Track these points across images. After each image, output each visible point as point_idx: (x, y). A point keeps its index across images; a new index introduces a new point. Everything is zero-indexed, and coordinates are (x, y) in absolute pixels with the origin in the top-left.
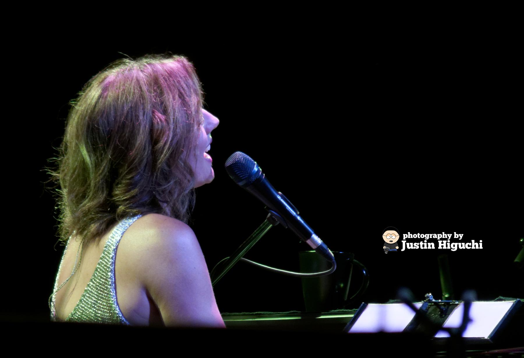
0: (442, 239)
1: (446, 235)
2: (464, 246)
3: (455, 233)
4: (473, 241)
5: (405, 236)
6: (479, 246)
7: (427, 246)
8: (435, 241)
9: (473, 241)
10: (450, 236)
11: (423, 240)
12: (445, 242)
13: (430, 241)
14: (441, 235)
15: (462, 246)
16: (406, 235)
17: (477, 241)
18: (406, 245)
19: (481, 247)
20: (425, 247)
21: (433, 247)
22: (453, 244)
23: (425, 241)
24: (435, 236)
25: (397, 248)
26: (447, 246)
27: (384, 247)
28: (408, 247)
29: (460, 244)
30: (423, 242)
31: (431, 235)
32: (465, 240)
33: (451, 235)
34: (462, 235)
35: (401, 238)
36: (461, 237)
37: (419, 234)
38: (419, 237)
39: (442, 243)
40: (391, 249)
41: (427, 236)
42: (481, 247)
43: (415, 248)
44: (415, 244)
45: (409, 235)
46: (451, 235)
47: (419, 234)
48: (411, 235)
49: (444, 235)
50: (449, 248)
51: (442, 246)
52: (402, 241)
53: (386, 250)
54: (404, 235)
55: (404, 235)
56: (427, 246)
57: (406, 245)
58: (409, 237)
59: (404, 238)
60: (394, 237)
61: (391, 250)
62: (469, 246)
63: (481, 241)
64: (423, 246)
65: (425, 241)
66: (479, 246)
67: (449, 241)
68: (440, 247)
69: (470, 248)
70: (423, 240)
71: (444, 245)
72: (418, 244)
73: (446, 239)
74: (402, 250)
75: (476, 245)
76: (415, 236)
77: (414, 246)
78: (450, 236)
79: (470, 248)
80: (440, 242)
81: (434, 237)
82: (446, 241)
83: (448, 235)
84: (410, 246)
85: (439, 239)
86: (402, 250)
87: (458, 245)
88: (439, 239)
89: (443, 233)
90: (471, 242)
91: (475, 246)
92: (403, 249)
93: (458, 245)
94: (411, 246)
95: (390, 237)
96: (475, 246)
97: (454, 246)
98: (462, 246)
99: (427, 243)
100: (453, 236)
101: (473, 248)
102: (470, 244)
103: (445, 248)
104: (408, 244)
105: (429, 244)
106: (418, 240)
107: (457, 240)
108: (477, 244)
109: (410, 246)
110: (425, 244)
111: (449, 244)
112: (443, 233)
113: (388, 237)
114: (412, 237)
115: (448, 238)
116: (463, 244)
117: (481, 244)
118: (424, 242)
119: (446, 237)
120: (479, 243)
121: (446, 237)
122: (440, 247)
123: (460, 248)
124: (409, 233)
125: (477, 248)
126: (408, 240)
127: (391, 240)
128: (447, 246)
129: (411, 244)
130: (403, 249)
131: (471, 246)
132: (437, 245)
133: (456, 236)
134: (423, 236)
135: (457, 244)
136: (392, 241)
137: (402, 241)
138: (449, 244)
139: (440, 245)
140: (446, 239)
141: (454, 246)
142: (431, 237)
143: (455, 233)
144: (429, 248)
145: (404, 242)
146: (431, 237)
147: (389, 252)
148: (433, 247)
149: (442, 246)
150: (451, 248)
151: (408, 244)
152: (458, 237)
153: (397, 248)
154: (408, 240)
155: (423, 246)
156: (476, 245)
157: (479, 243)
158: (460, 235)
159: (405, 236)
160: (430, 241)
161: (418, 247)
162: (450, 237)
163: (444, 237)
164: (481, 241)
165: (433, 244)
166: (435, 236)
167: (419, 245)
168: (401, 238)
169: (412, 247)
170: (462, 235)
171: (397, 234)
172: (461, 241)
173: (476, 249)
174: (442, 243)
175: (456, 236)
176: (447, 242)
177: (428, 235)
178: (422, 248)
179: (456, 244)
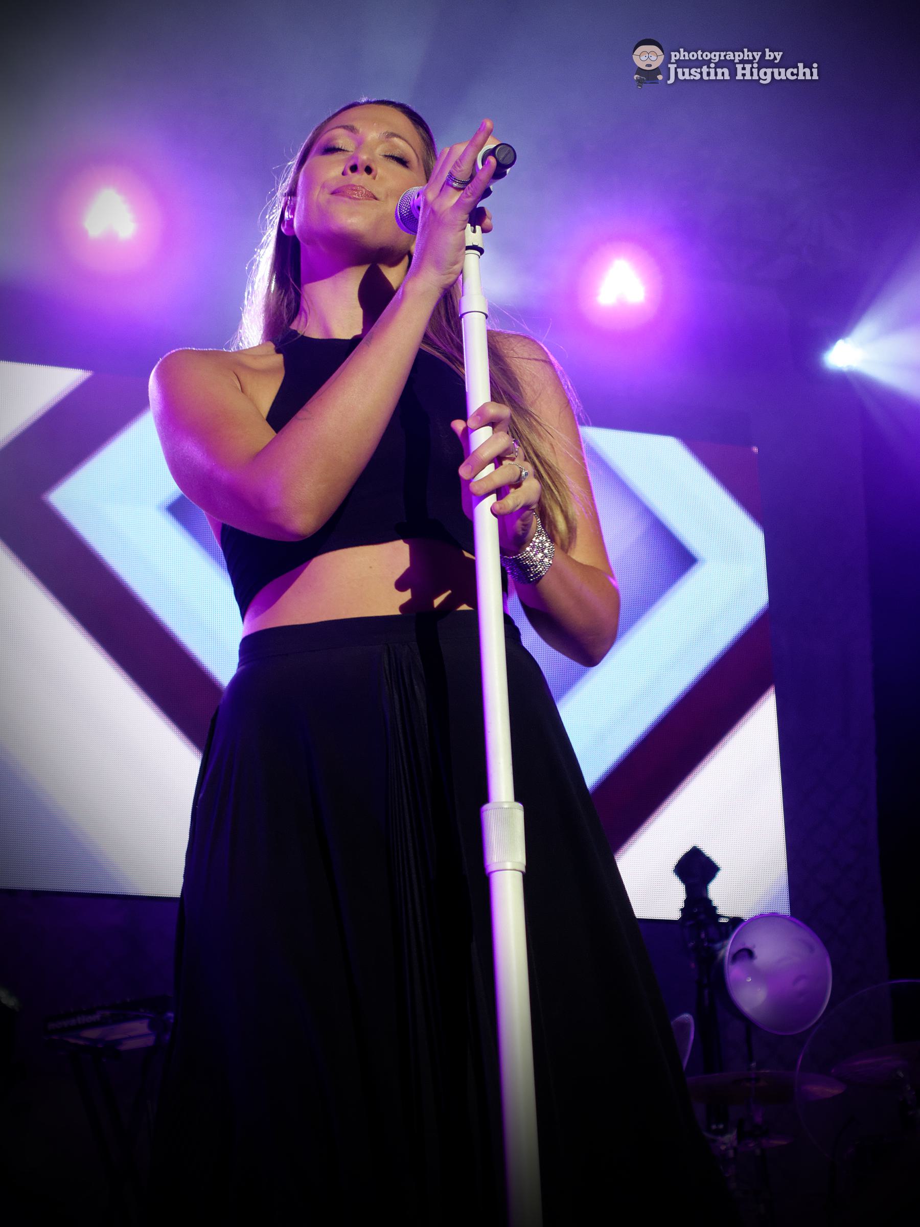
19: (815, 77)
20: (712, 77)
21: (727, 77)
28: (681, 77)
43: (692, 77)
50: (755, 77)
53: (638, 81)
68: (739, 77)
69: (795, 77)
74: (669, 82)
79: (795, 77)
86: (669, 82)
92: (672, 80)
101: (801, 77)
103: (748, 77)
123: (777, 77)
125: (808, 77)
130: (672, 80)
144: (720, 77)
150: (760, 78)
161: (698, 77)
169: (687, 77)
178: (705, 77)
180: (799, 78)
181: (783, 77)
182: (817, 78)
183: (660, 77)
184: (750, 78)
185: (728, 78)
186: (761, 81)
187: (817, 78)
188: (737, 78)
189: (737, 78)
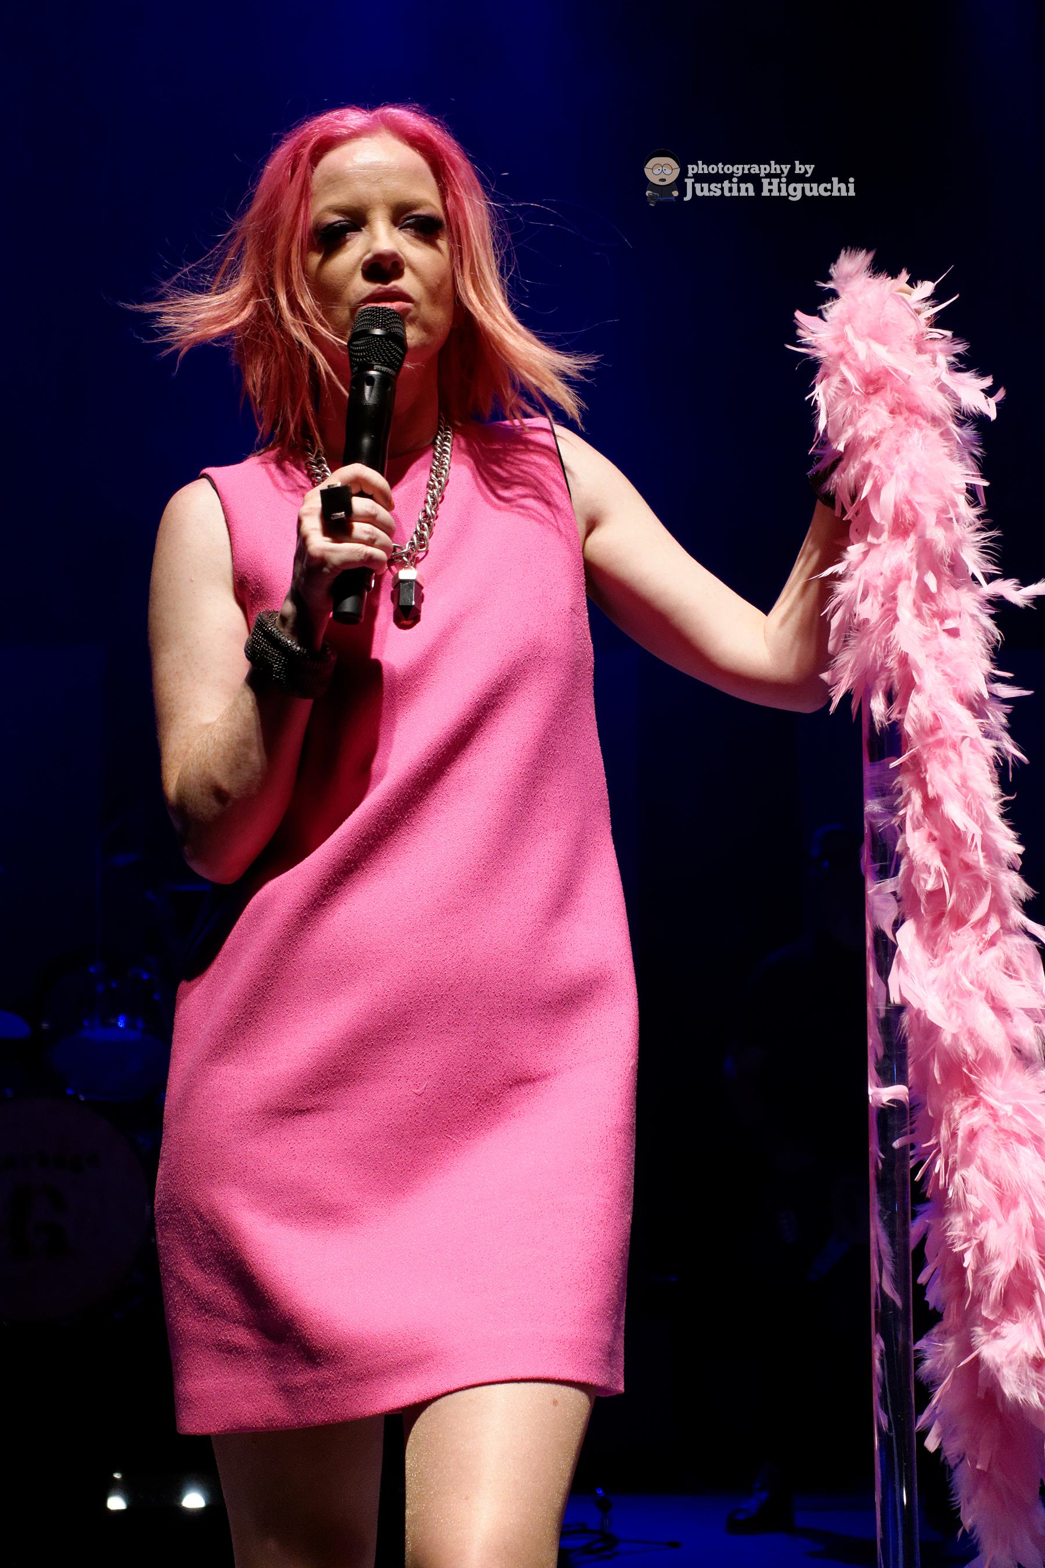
0: (769, 176)
1: (778, 166)
2: (816, 190)
3: (797, 162)
4: (835, 180)
6: (848, 190)
7: (739, 190)
8: (755, 180)
9: (835, 180)
10: (786, 168)
11: (729, 177)
12: (775, 181)
13: (744, 179)
14: (767, 167)
15: (811, 190)
16: (695, 166)
17: (844, 180)
19: (852, 193)
20: (735, 193)
21: (752, 193)
22: (792, 186)
23: (735, 180)
24: (755, 169)
25: (676, 193)
26: (780, 190)
27: (648, 193)
28: (699, 193)
29: (807, 186)
30: (730, 182)
31: (747, 167)
32: (818, 178)
33: (789, 166)
34: (813, 166)
35: (684, 173)
36: (810, 171)
37: (720, 165)
38: (721, 172)
39: (770, 184)
40: (661, 196)
41: (738, 170)
42: (852, 193)
43: (712, 194)
44: (713, 186)
45: (701, 168)
46: (789, 166)
47: (720, 165)
48: (705, 166)
49: (774, 167)
50: (784, 193)
51: (770, 191)
52: (686, 180)
53: (651, 197)
54: (690, 167)
55: (690, 167)
56: (739, 190)
58: (700, 172)
59: (690, 173)
60: (668, 171)
61: (662, 199)
62: (826, 190)
63: (852, 180)
64: (730, 190)
65: (735, 180)
66: (848, 190)
67: (784, 180)
68: (765, 193)
69: (829, 193)
70: (729, 177)
71: (775, 187)
72: (719, 185)
73: (778, 176)
74: (686, 199)
75: (841, 189)
77: (710, 190)
78: (786, 168)
79: (829, 193)
80: (765, 181)
81: (752, 171)
82: (778, 180)
83: (783, 167)
84: (702, 190)
85: (762, 175)
86: (686, 199)
87: (803, 189)
88: (762, 175)
89: (773, 162)
90: (832, 182)
91: (839, 190)
92: (688, 197)
93: (803, 189)
94: (704, 190)
95: (661, 170)
96: (839, 190)
97: (795, 189)
98: (811, 190)
99: (738, 183)
100: (793, 169)
101: (835, 193)
102: (829, 186)
103: (775, 193)
104: (698, 186)
105: (743, 186)
106: (719, 178)
107: (801, 179)
108: (843, 186)
109: (702, 190)
110: (735, 186)
111: (783, 186)
112: (773, 162)
113: (656, 171)
114: (706, 172)
115: (782, 172)
116: (814, 186)
117: (851, 186)
118: (731, 182)
119: (779, 171)
120: (847, 183)
121: (779, 171)
122: (765, 193)
123: (808, 193)
124: (700, 162)
125: (844, 193)
126: (699, 178)
127: (663, 176)
128: (780, 190)
129: (705, 186)
130: (688, 197)
131: (831, 191)
132: (758, 188)
133: (799, 168)
134: (729, 169)
135: (801, 185)
136: (663, 180)
137: (686, 180)
138: (783, 186)
140: (778, 176)
141: (795, 189)
142: (746, 171)
143: (797, 162)
144: (743, 193)
145: (689, 182)
146: (746, 171)
147: (658, 203)
149: (770, 191)
150: (789, 195)
152: (803, 171)
153: (676, 193)
154: (699, 178)
155: (730, 190)
156: (841, 189)
157: (847, 183)
158: (807, 166)
160: (744, 179)
161: (719, 193)
162: (786, 171)
163: (773, 171)
165: (750, 186)
166: (755, 169)
167: (722, 189)
168: (684, 173)
169: (706, 193)
170: (813, 166)
172: (810, 180)
173: (840, 197)
174: (770, 184)
175: (799, 168)
176: (781, 182)
177: (741, 167)
178: (727, 194)
179: (799, 186)
180: (834, 194)
181: (815, 193)
182: (853, 194)
184: (778, 194)
185: (753, 194)
186: (790, 198)
187: (853, 194)
188: (763, 194)
189: (763, 194)
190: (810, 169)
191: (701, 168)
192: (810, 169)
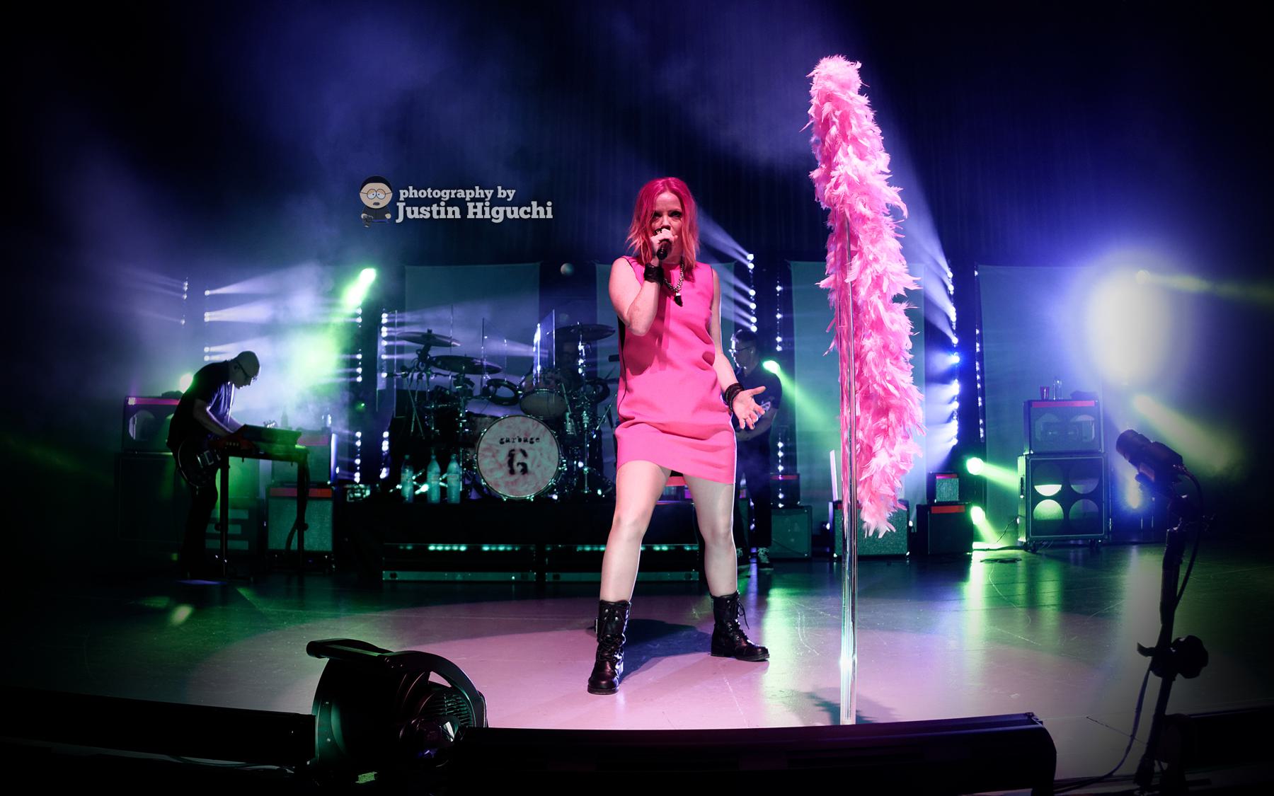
0: (474, 200)
2: (517, 213)
4: (534, 204)
5: (403, 194)
7: (446, 213)
9: (534, 204)
13: (451, 203)
17: (542, 204)
18: (405, 212)
23: (443, 204)
25: (388, 216)
26: (483, 213)
28: (410, 216)
31: (453, 192)
32: (518, 202)
35: (396, 198)
36: (511, 196)
37: (429, 190)
39: (475, 207)
42: (550, 216)
44: (422, 209)
45: (412, 193)
47: (429, 190)
51: (475, 214)
53: (366, 219)
56: (446, 213)
57: (405, 212)
59: (402, 198)
60: (382, 196)
62: (526, 213)
63: (549, 203)
64: (439, 213)
65: (443, 204)
67: (487, 204)
73: (482, 200)
75: (539, 212)
76: (422, 194)
92: (400, 220)
97: (498, 212)
100: (496, 193)
102: (528, 209)
104: (408, 209)
108: (541, 209)
110: (442, 210)
111: (487, 209)
113: (371, 196)
116: (515, 209)
117: (549, 210)
120: (545, 206)
126: (410, 202)
127: (376, 200)
128: (483, 213)
130: (400, 220)
138: (487, 209)
139: (471, 210)
140: (482, 200)
141: (498, 212)
145: (401, 205)
148: (458, 216)
149: (475, 214)
151: (408, 209)
155: (439, 213)
157: (545, 206)
159: (403, 194)
160: (451, 203)
162: (489, 196)
164: (549, 203)
167: (431, 212)
168: (396, 198)
171: (387, 189)
172: (511, 204)
174: (475, 207)
183: (388, 216)
190: (511, 193)
191: (412, 193)
192: (511, 193)
